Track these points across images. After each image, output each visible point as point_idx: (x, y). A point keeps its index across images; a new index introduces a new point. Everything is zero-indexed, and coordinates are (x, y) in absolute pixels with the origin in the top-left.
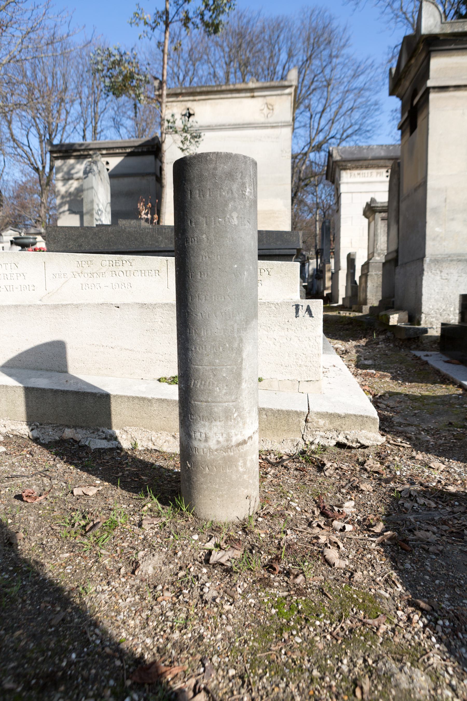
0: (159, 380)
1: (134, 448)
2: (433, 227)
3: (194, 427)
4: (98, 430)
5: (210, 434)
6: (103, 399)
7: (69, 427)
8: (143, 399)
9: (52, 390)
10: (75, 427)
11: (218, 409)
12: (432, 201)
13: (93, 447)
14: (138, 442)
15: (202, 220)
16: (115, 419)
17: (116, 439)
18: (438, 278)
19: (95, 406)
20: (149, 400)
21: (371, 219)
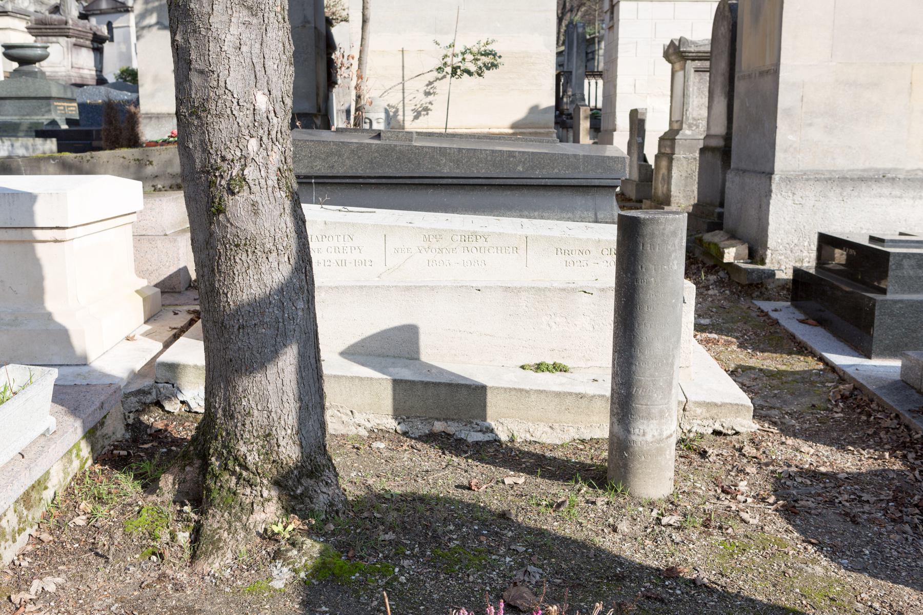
0: (523, 367)
1: (512, 440)
2: (785, 135)
3: (633, 425)
4: (471, 423)
5: (648, 430)
6: (480, 391)
7: (438, 420)
8: (521, 390)
9: (422, 382)
10: (445, 420)
11: (655, 411)
12: (785, 100)
13: (470, 440)
14: (515, 434)
15: (651, 267)
16: (491, 411)
17: (492, 431)
18: (790, 202)
19: (469, 398)
20: (527, 392)
21: (677, 66)
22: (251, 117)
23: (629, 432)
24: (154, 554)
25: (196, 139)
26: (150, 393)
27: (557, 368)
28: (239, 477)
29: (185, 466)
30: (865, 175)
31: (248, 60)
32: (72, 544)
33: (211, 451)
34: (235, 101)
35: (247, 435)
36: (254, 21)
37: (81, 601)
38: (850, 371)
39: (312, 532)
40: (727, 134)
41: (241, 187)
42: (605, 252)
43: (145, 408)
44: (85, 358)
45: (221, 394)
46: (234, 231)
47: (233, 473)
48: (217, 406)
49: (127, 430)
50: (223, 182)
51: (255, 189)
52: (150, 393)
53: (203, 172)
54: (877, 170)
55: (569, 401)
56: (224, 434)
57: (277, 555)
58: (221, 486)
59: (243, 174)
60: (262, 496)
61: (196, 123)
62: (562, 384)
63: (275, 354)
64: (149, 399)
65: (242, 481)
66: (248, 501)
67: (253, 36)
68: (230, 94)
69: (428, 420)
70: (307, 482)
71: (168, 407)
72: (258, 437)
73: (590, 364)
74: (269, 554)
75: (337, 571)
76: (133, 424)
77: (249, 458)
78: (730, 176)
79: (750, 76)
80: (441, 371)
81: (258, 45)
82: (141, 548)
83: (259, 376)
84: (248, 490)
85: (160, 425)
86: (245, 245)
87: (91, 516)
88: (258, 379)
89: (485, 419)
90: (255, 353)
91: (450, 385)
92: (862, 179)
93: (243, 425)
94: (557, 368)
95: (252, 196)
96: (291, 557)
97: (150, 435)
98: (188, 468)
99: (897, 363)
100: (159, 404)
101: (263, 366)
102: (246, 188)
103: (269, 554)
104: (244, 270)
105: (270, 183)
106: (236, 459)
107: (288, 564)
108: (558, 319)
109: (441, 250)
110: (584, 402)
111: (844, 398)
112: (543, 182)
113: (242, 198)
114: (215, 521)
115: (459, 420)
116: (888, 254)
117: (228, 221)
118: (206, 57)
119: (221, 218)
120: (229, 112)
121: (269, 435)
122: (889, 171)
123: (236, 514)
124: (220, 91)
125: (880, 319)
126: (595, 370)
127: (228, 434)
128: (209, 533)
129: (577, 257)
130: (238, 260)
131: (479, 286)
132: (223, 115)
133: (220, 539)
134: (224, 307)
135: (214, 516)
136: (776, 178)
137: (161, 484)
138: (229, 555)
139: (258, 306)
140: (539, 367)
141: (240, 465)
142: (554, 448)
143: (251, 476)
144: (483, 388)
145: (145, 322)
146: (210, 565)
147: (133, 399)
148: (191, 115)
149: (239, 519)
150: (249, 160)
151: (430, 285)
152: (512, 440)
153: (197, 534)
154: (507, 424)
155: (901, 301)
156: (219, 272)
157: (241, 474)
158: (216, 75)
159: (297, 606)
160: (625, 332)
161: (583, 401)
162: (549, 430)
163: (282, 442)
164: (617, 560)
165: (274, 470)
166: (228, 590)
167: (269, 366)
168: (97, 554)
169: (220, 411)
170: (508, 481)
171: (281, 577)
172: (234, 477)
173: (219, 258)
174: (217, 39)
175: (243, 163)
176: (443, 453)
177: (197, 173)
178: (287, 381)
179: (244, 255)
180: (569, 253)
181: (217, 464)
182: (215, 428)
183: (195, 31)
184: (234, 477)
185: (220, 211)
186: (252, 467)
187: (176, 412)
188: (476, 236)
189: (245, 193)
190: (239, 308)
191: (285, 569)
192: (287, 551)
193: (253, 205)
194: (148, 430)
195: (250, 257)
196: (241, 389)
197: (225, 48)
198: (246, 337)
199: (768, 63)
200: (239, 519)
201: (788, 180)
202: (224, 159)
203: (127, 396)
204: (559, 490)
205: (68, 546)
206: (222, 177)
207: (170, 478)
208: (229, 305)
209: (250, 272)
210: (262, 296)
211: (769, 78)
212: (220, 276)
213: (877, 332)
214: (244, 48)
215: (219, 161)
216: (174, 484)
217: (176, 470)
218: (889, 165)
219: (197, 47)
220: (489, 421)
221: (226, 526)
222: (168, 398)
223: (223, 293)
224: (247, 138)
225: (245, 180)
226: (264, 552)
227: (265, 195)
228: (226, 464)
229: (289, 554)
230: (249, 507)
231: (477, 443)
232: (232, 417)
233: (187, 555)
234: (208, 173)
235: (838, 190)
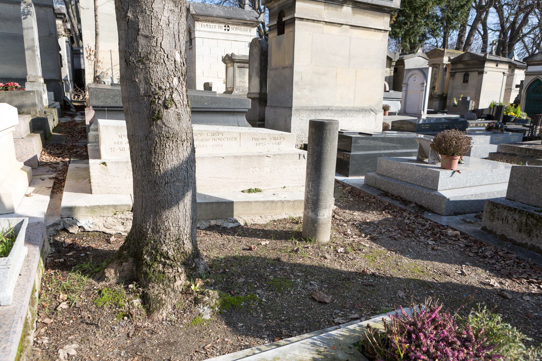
0: (243, 191)
1: (246, 224)
2: (296, 92)
3: (319, 212)
4: (227, 219)
5: (325, 214)
6: (230, 205)
7: (212, 219)
8: (248, 202)
9: (205, 203)
10: (216, 219)
11: (328, 205)
12: (296, 78)
13: (229, 227)
14: (247, 222)
15: (329, 143)
16: (235, 213)
17: (237, 222)
18: (298, 119)
19: (226, 207)
20: (251, 202)
21: (229, 65)
22: (173, 65)
23: (317, 215)
24: (124, 316)
25: (141, 76)
26: (60, 224)
27: (257, 191)
28: (164, 264)
29: (122, 262)
30: (323, 108)
31: (172, 32)
32: (68, 321)
33: (144, 252)
34: (166, 55)
35: (167, 241)
36: (177, 10)
37: (98, 355)
38: (345, 181)
39: (213, 286)
40: (260, 94)
41: (172, 105)
42: (272, 139)
43: (57, 232)
44: (13, 209)
45: (151, 221)
46: (167, 129)
47: (161, 262)
48: (148, 227)
49: (51, 247)
50: (160, 102)
51: (179, 106)
52: (60, 224)
53: (146, 96)
54: (326, 106)
55: (268, 205)
56: (152, 242)
57: (196, 301)
58: (154, 270)
59: (172, 97)
60: (178, 272)
61: (141, 67)
62: (263, 197)
63: (184, 195)
64: (60, 227)
65: (166, 266)
66: (172, 276)
67: (175, 19)
68: (163, 51)
69: (208, 220)
70: (196, 260)
71: (71, 230)
72: (173, 241)
73: (269, 187)
74: (190, 301)
75: (233, 303)
76: (53, 243)
77: (170, 253)
78: (267, 109)
79: (276, 69)
80: (211, 197)
81: (177, 24)
82: (114, 314)
83: (175, 209)
84: (171, 270)
85: (69, 241)
86: (172, 137)
87: (69, 301)
88: (174, 210)
89: (233, 217)
90: (173, 196)
91: (218, 203)
92: (322, 110)
93: (165, 236)
94: (257, 191)
95: (177, 110)
96: (206, 301)
97: (66, 247)
98: (124, 264)
99: (363, 178)
100: (65, 230)
101: (177, 203)
102: (174, 105)
103: (190, 301)
104: (170, 151)
105: (184, 102)
106: (162, 254)
107: (207, 305)
108: (257, 169)
109: (202, 140)
110: (274, 204)
111: (350, 193)
112: (216, 110)
113: (172, 110)
114: (155, 290)
115: (221, 219)
116: (352, 137)
117: (164, 124)
118: (150, 28)
119: (159, 122)
120: (163, 62)
121: (179, 239)
122: (330, 107)
123: (166, 284)
124: (158, 49)
125: (352, 162)
126: (298, 191)
127: (155, 242)
128: (154, 297)
129: (261, 141)
130: (167, 146)
131: (223, 156)
132: (159, 63)
133: (162, 299)
134: (157, 173)
135: (153, 287)
136: (293, 109)
137: (107, 275)
138: (169, 307)
139: (176, 170)
140: (250, 191)
141: (164, 258)
142: (265, 226)
143: (172, 262)
144: (232, 203)
145: (30, 185)
146: (161, 314)
147: (52, 229)
148: (138, 62)
149: (169, 286)
150: (174, 90)
151: (201, 156)
152: (246, 224)
153: (145, 299)
154: (243, 217)
155: (358, 155)
156: (155, 153)
157: (166, 262)
158: (155, 39)
159: (226, 326)
160: (316, 173)
161: (273, 204)
162: (260, 218)
163: (185, 242)
164: (342, 272)
165: (182, 257)
166: (182, 326)
167: (180, 203)
168: (87, 324)
169: (150, 230)
170: (263, 243)
171: (206, 313)
172: (160, 265)
173: (156, 145)
174: (157, 18)
175: (171, 91)
176: (222, 235)
177: (141, 96)
178: (188, 210)
179: (171, 143)
180: (258, 139)
181: (148, 259)
182: (146, 240)
183: (142, 12)
184: (160, 265)
185: (159, 118)
186: (172, 258)
187: (76, 233)
188: (218, 133)
189: (174, 108)
190: (166, 173)
191: (206, 308)
192: (203, 298)
193: (178, 115)
194: (63, 245)
195: (174, 144)
196: (164, 217)
197: (161, 24)
198: (169, 188)
199: (287, 63)
200: (169, 286)
201: (297, 110)
202: (160, 88)
203: (48, 228)
204: (288, 245)
205: (66, 323)
206: (159, 99)
207: (113, 271)
208: (160, 171)
209: (173, 152)
210: (178, 165)
211: (288, 70)
212: (156, 155)
213: (350, 167)
214: (171, 25)
215: (157, 89)
216: (116, 273)
217: (115, 265)
218: (330, 105)
219: (144, 22)
220: (235, 217)
221: (163, 291)
222: (71, 226)
223: (157, 164)
224: (173, 77)
225: (173, 100)
226: (187, 301)
227: (183, 110)
228: (155, 258)
229: (205, 299)
230: (173, 279)
231: (232, 228)
232: (158, 232)
233: (144, 312)
234: (150, 96)
235: (314, 114)
